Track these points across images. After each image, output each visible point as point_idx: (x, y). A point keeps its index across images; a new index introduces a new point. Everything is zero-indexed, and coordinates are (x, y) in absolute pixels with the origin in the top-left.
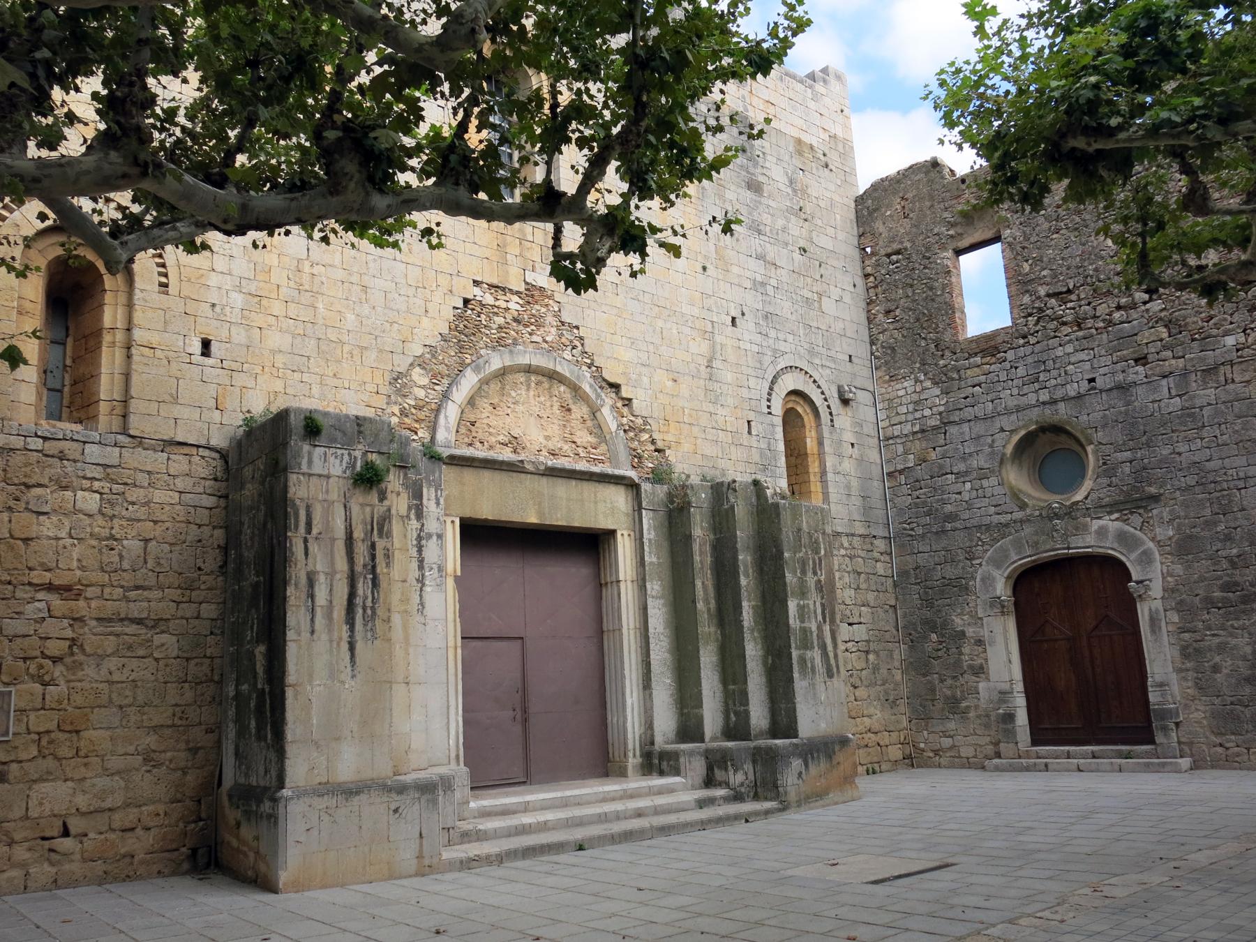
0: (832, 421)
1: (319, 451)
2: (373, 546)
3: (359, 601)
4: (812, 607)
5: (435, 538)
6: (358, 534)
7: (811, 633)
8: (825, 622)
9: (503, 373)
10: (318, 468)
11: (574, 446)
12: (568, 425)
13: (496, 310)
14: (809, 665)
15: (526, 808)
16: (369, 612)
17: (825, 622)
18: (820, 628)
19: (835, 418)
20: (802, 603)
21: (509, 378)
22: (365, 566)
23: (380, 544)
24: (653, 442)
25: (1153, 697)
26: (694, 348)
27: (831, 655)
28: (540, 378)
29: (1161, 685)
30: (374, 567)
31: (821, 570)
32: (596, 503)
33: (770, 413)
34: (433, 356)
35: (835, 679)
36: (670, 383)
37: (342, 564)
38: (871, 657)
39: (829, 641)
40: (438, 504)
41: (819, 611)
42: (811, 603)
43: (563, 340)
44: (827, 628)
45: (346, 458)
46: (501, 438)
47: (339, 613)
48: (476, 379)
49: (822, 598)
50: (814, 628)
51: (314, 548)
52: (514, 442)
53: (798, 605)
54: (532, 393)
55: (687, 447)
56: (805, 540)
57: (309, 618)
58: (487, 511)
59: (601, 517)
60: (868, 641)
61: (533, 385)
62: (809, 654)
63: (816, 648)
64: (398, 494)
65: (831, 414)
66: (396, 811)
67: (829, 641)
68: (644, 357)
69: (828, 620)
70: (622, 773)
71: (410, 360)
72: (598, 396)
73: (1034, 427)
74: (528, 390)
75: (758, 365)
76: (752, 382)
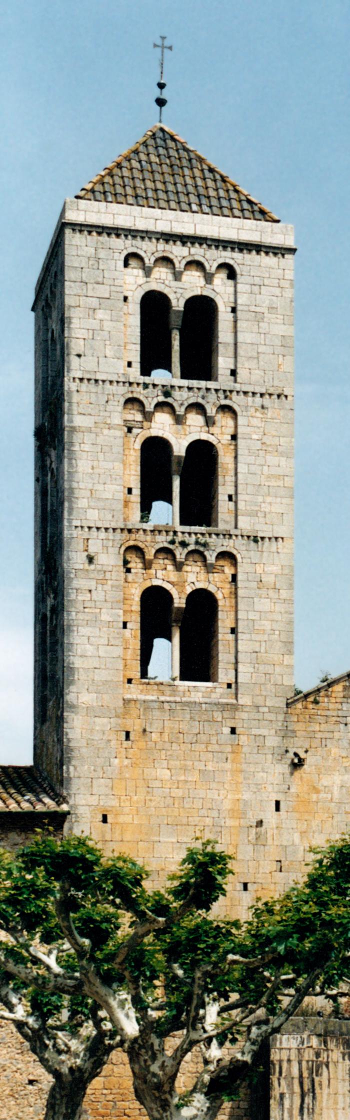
1: (285, 1037)
2: (313, 1081)
3: (305, 1105)
10: (284, 1045)
16: (311, 1110)
22: (309, 1090)
23: (317, 1079)
37: (297, 1088)
45: (299, 1039)
47: (296, 1112)
51: (283, 1082)
57: (281, 1113)
64: (332, 1051)
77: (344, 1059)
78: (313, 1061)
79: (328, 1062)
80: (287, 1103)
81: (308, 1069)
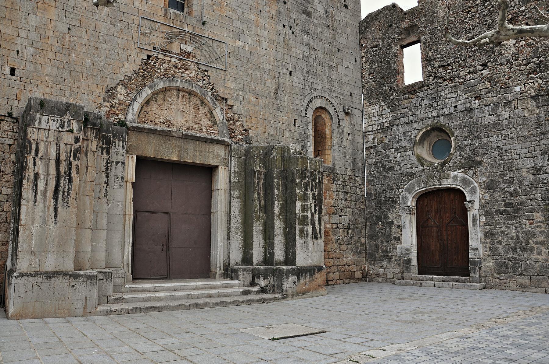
0: (339, 122)
1: (45, 118)
2: (70, 164)
4: (309, 206)
5: (120, 164)
6: (63, 157)
7: (308, 218)
8: (316, 213)
9: (164, 91)
10: (44, 125)
11: (200, 126)
12: (197, 116)
13: (164, 61)
14: (305, 233)
15: (155, 290)
17: (316, 213)
18: (312, 216)
19: (340, 121)
20: (304, 203)
21: (168, 93)
22: (65, 172)
23: (74, 163)
24: (243, 126)
25: (471, 255)
26: (268, 84)
27: (318, 229)
28: (184, 93)
29: (475, 249)
30: (70, 173)
31: (316, 189)
32: (209, 152)
33: (306, 117)
34: (129, 81)
35: (319, 240)
36: (253, 100)
37: (53, 171)
38: (350, 231)
39: (317, 222)
40: (123, 148)
41: (313, 208)
42: (309, 204)
43: (199, 76)
44: (316, 216)
45: (59, 122)
46: (162, 120)
47: (50, 193)
48: (150, 92)
49: (315, 202)
50: (309, 215)
51: (38, 162)
52: (168, 122)
53: (302, 205)
54: (180, 100)
55: (260, 129)
56: (308, 174)
57: (33, 195)
58: (150, 153)
59: (211, 159)
60: (349, 224)
61: (180, 96)
62: (305, 227)
63: (310, 225)
64: (92, 141)
65: (339, 119)
66: (73, 286)
67: (317, 222)
68: (241, 87)
69: (317, 212)
70: (214, 277)
71: (117, 82)
72: (214, 103)
73: (429, 128)
74: (178, 98)
75: (302, 94)
76: (298, 102)
77: (102, 153)
78: (71, 145)
79: (87, 151)
80: (41, 185)
81: (66, 152)
